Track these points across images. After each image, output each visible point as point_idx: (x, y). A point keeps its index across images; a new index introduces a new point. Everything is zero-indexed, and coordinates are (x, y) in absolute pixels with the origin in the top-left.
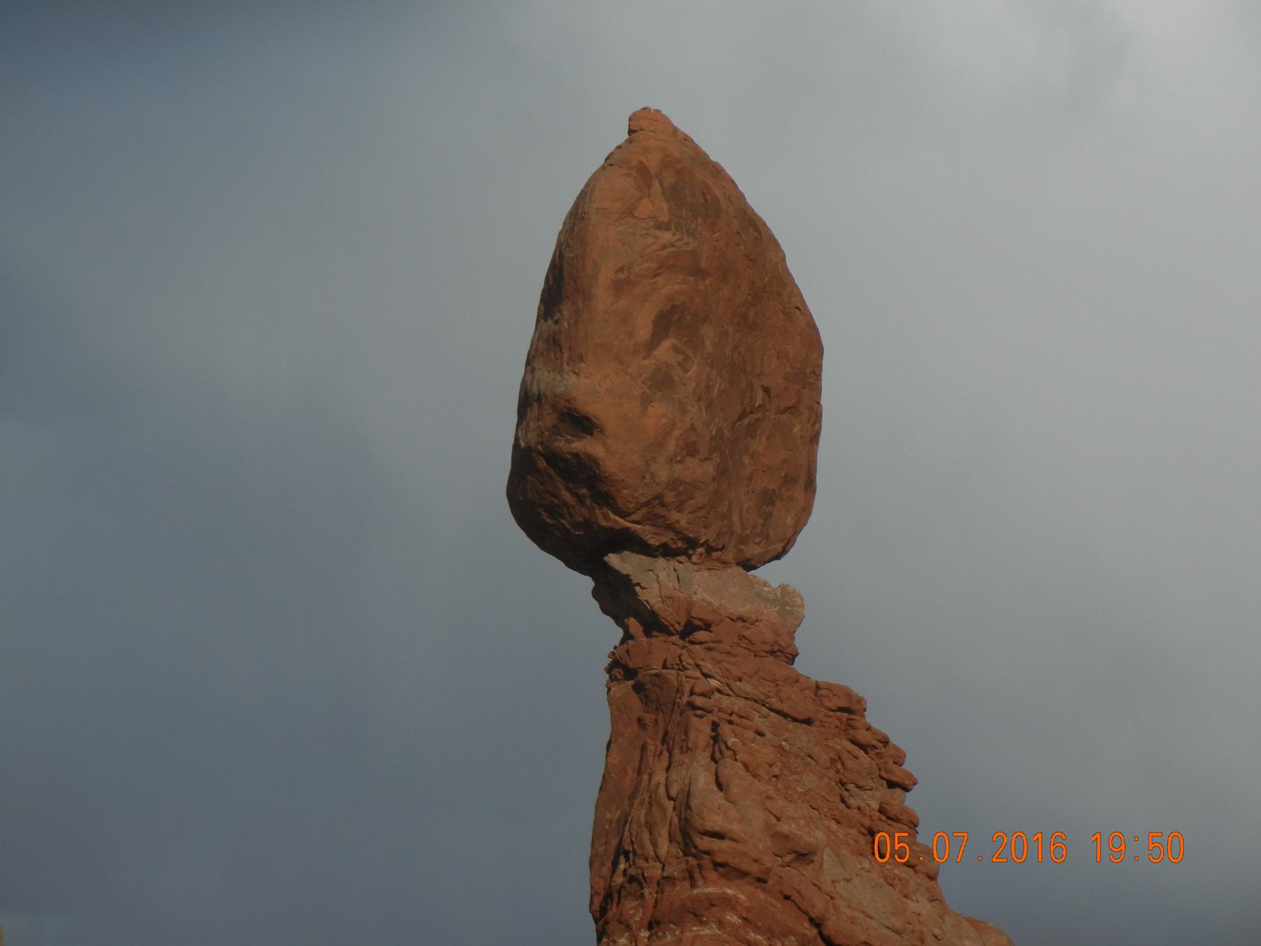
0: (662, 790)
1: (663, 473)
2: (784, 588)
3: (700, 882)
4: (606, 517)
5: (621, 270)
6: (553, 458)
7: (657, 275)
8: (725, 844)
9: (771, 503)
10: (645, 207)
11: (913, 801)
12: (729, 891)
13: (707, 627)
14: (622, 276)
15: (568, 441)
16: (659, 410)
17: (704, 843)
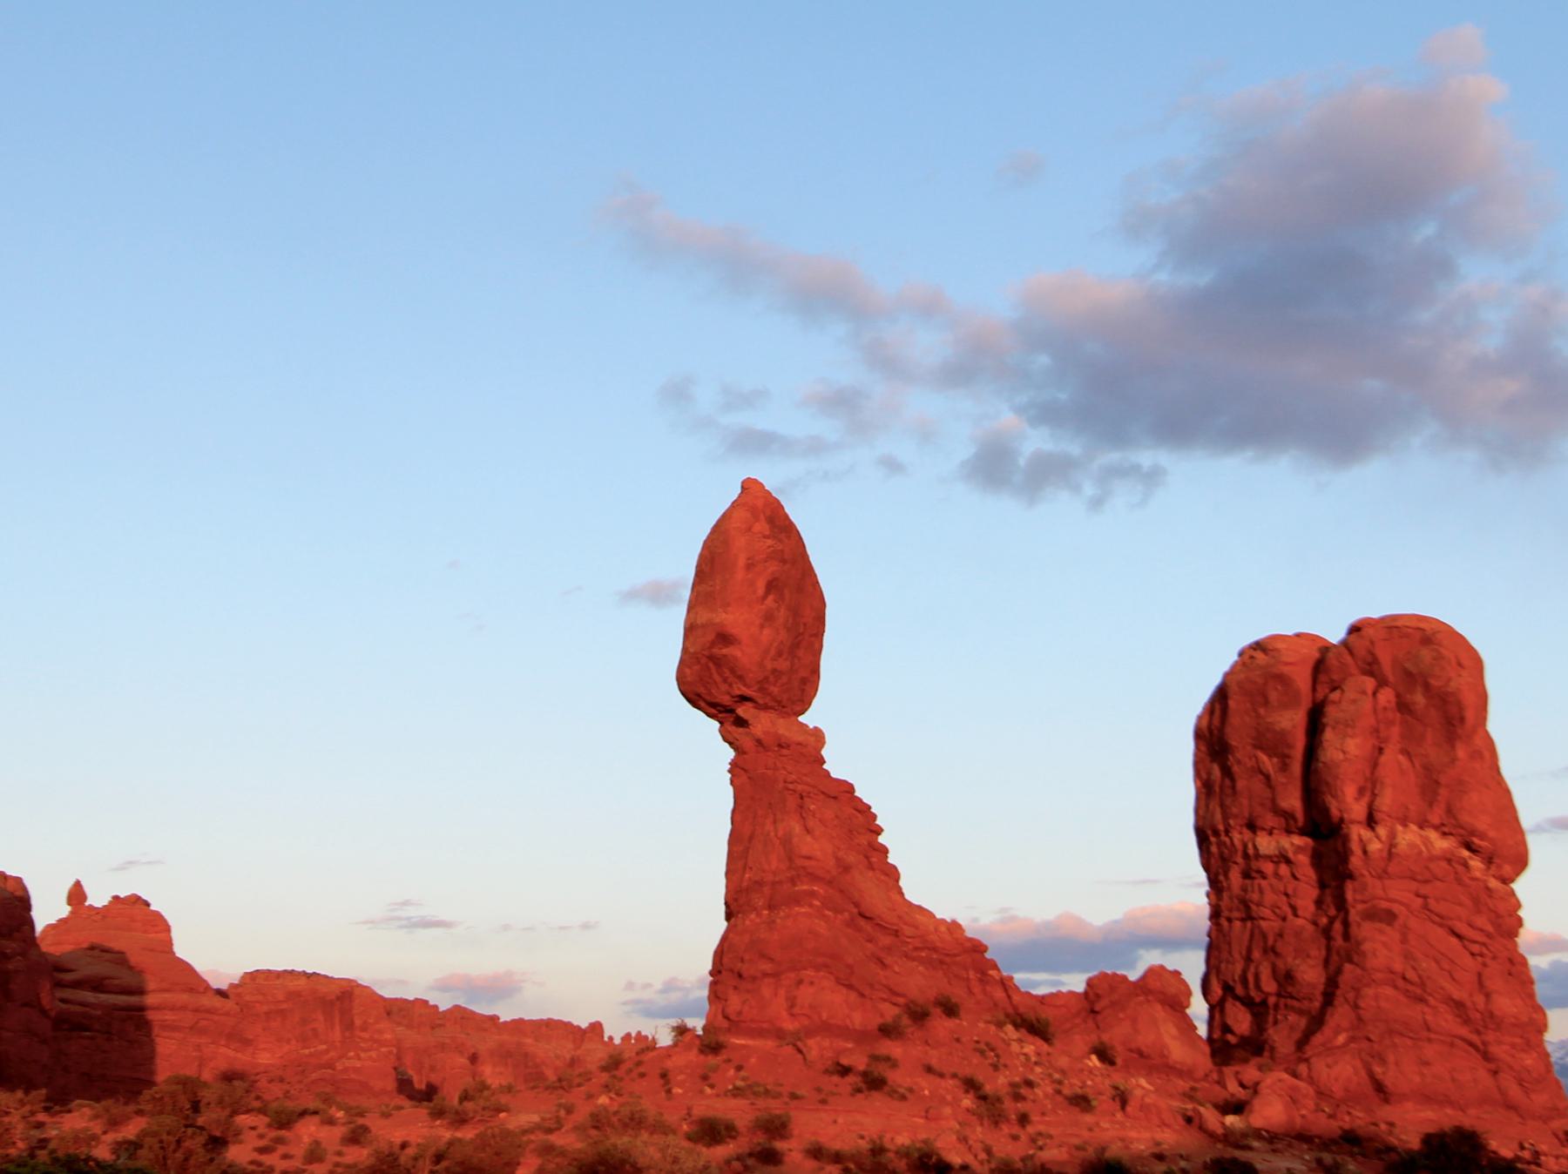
0: (772, 834)
1: (769, 665)
2: (816, 728)
3: (799, 883)
4: (739, 689)
5: (749, 559)
6: (711, 658)
7: (766, 562)
8: (813, 863)
9: (805, 684)
10: (757, 527)
11: (882, 839)
12: (815, 888)
13: (788, 747)
14: (750, 562)
15: (721, 649)
16: (767, 632)
17: (800, 862)
